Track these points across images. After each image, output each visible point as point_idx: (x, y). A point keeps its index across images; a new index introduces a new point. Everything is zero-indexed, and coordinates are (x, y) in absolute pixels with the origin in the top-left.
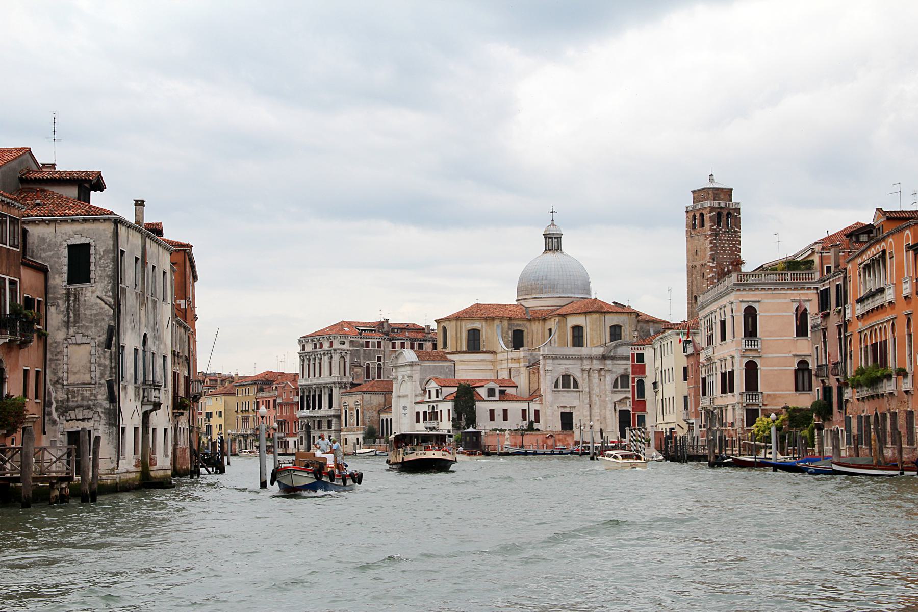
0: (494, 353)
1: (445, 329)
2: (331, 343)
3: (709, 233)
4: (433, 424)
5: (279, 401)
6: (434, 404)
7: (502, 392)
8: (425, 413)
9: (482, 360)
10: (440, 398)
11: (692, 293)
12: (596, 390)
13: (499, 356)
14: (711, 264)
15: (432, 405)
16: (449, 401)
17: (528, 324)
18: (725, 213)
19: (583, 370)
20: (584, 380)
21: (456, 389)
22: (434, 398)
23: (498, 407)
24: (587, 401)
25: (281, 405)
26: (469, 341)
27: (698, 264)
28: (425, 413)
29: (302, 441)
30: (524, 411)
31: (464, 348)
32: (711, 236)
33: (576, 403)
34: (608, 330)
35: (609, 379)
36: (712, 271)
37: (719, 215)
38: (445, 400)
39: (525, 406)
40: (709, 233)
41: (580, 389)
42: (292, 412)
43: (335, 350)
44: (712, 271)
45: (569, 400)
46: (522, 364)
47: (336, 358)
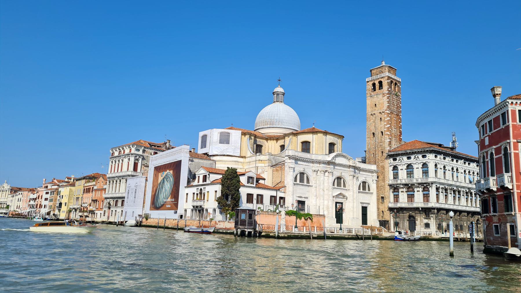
2: (131, 150)
3: (387, 92)
5: (95, 188)
6: (202, 187)
7: (257, 181)
9: (235, 161)
10: (208, 182)
14: (388, 112)
15: (200, 188)
16: (217, 183)
17: (265, 141)
18: (394, 82)
21: (221, 176)
22: (201, 182)
23: (255, 192)
25: (96, 190)
29: (104, 213)
32: (388, 94)
34: (328, 145)
35: (331, 179)
36: (388, 116)
37: (392, 82)
38: (213, 183)
39: (274, 193)
40: (387, 92)
42: (101, 195)
43: (132, 154)
44: (388, 116)
45: (301, 192)
46: (267, 165)
47: (132, 159)
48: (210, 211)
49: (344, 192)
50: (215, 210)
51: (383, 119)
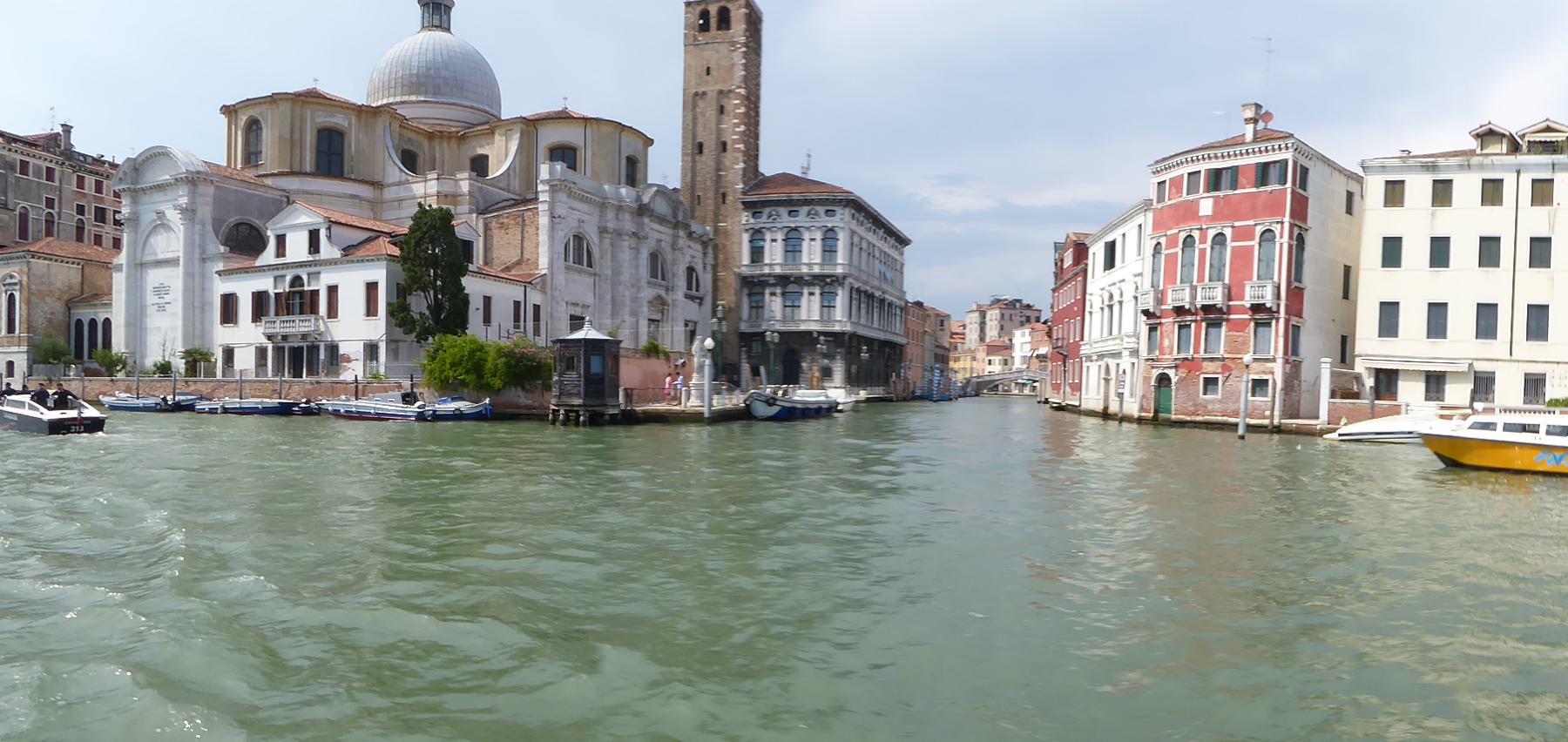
0: (377, 185)
1: (253, 127)
4: (299, 326)
8: (260, 299)
9: (353, 196)
11: (694, 137)
12: (626, 276)
13: (390, 193)
19: (603, 231)
20: (601, 251)
24: (609, 297)
26: (319, 153)
27: (712, 88)
28: (260, 299)
30: (517, 304)
31: (308, 167)
33: (589, 298)
34: (624, 162)
41: (596, 269)
48: (352, 348)
49: (663, 293)
50: (371, 350)
51: (728, 108)
